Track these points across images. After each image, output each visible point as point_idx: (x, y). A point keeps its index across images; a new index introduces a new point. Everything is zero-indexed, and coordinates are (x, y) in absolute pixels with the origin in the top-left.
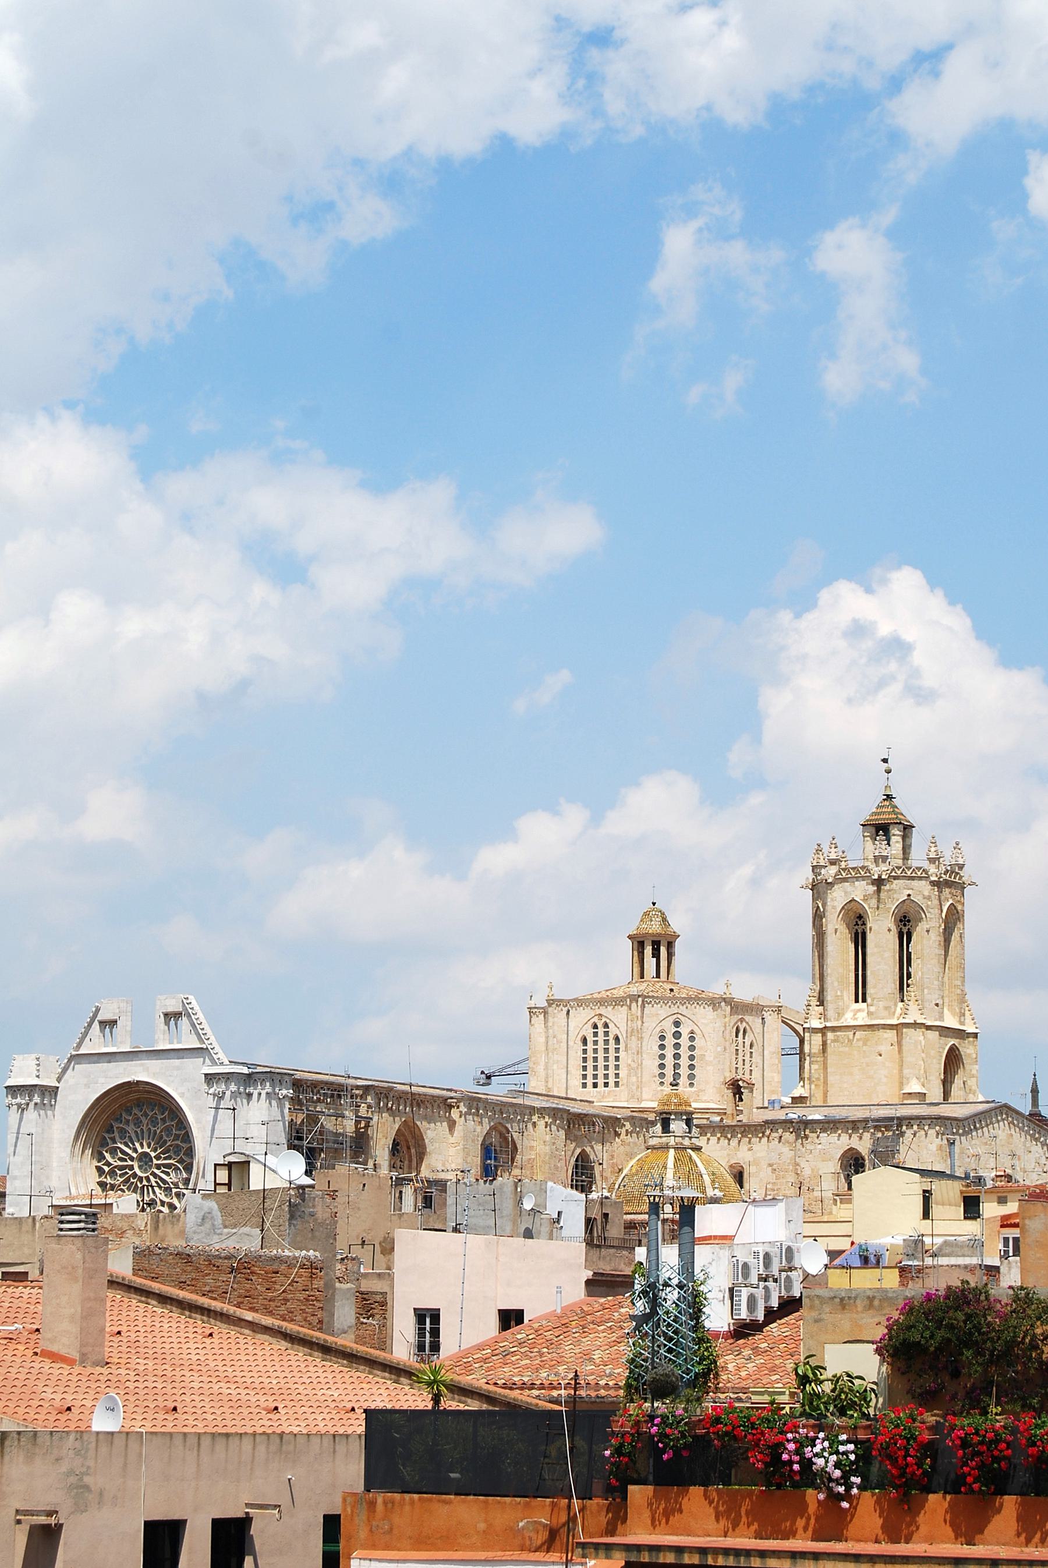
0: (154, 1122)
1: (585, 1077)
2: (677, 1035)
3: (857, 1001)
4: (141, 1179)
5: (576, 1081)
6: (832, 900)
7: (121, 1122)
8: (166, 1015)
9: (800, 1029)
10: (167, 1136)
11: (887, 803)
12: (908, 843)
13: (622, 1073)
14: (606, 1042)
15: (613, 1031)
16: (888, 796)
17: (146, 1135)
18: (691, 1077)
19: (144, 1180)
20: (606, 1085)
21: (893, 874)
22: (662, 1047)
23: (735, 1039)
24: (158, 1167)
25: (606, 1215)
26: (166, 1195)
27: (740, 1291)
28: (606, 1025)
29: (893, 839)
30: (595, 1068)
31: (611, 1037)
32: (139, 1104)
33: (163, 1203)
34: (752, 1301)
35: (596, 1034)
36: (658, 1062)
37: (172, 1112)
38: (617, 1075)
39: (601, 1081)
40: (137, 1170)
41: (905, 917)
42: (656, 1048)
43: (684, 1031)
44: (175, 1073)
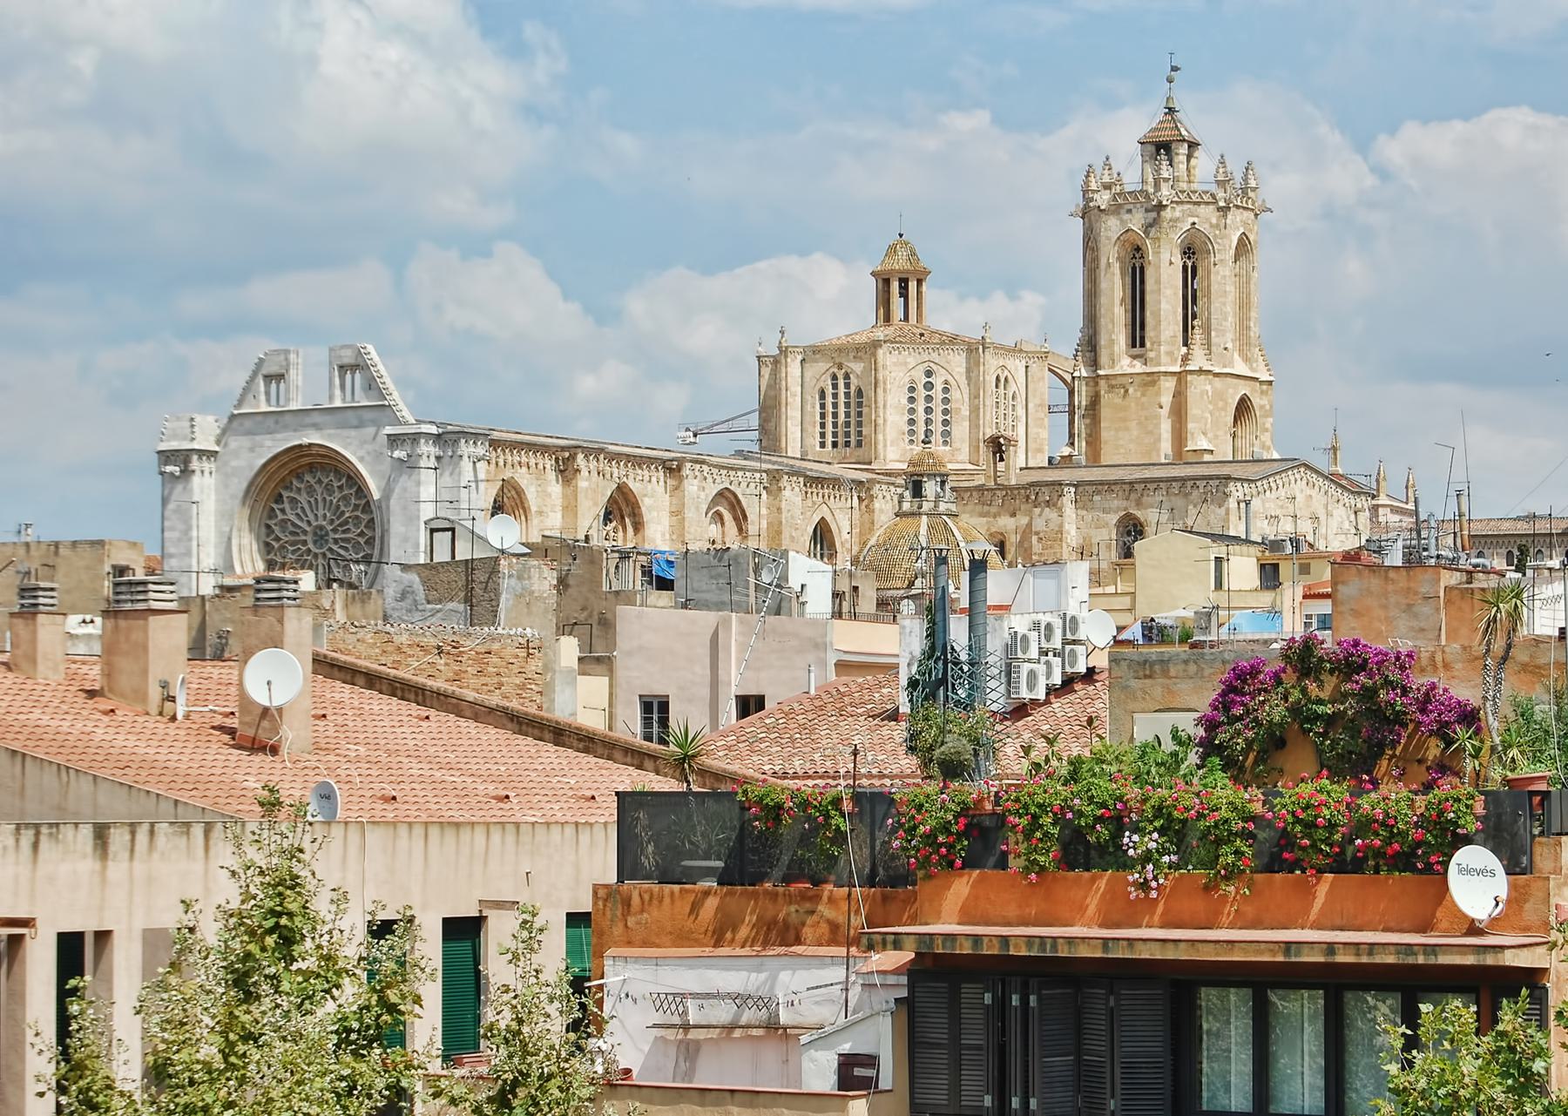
0: (329, 489)
2: (929, 386)
3: (1134, 346)
4: (316, 556)
6: (1106, 229)
7: (291, 490)
8: (341, 367)
9: (1068, 378)
10: (345, 506)
14: (847, 395)
16: (1170, 109)
17: (321, 505)
18: (946, 434)
19: (320, 556)
21: (1176, 199)
22: (912, 400)
23: (995, 390)
24: (336, 541)
25: (856, 589)
27: (1019, 667)
32: (311, 468)
35: (835, 386)
36: (906, 417)
37: (349, 477)
40: (311, 546)
41: (1189, 249)
42: (904, 401)
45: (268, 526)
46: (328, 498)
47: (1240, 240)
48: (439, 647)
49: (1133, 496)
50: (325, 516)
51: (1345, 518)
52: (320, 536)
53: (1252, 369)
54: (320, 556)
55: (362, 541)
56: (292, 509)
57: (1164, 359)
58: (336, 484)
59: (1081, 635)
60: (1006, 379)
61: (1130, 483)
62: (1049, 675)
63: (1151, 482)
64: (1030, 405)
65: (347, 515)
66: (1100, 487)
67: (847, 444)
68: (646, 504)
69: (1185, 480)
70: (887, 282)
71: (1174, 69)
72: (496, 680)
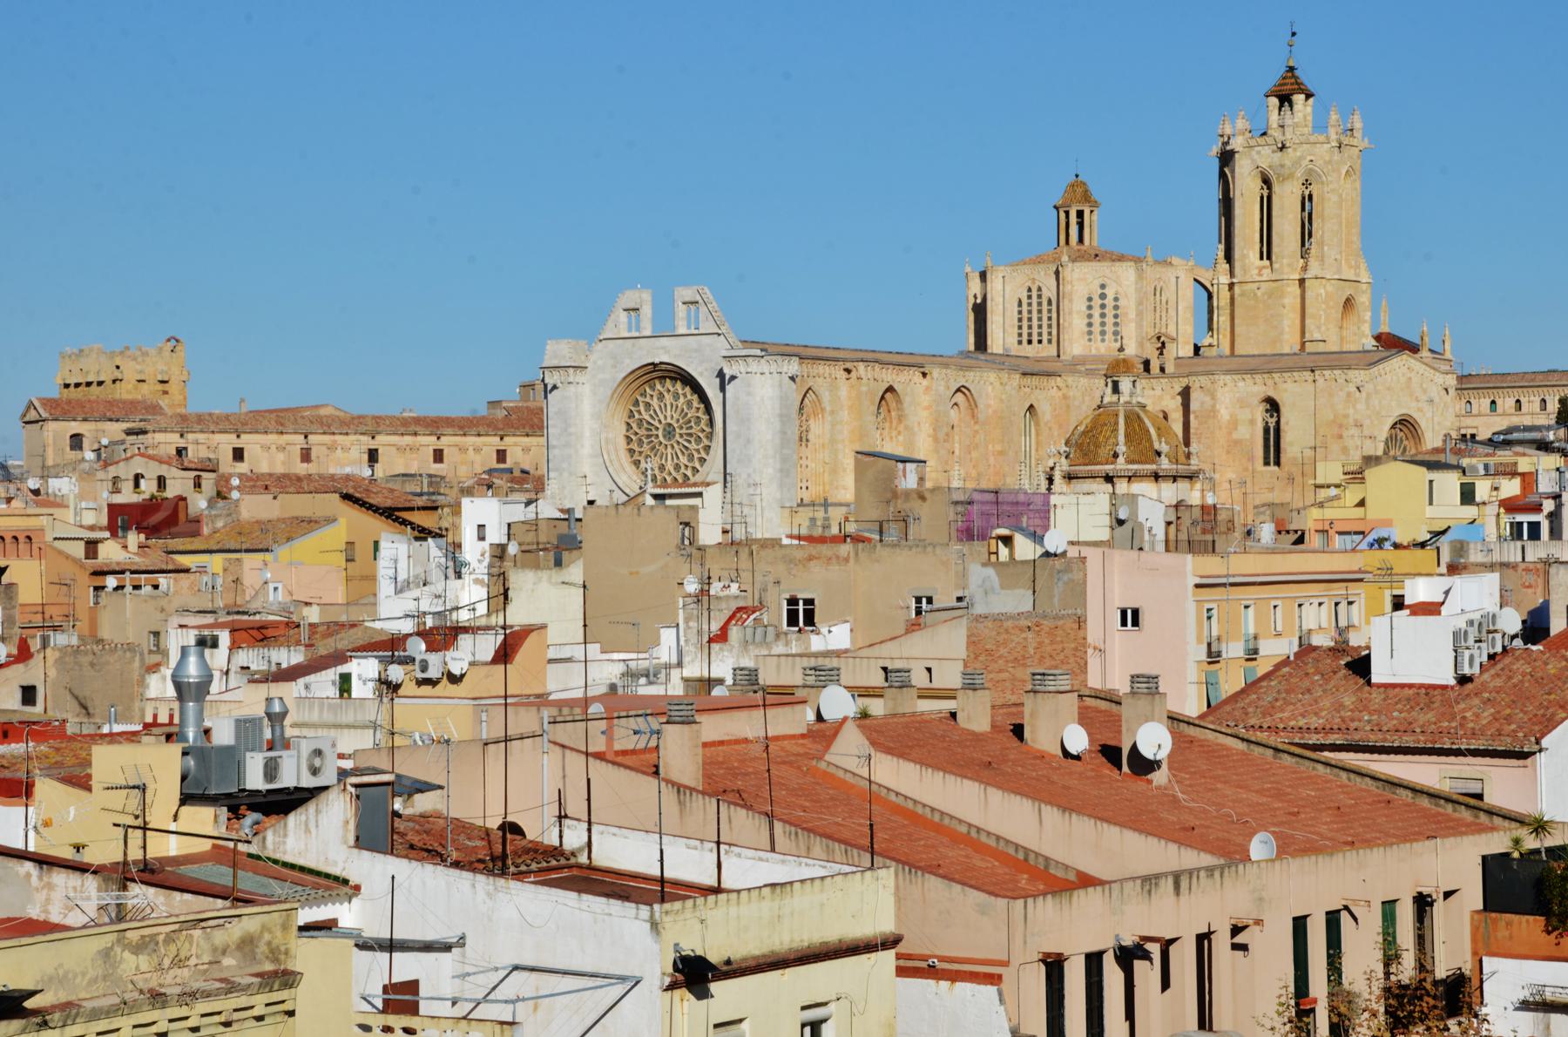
1: (1020, 335)
2: (1103, 296)
9: (1209, 286)
11: (1289, 74)
14: (1040, 304)
15: (1046, 294)
17: (669, 407)
19: (669, 447)
20: (1040, 342)
22: (1090, 307)
28: (1039, 289)
29: (1296, 107)
35: (1030, 297)
36: (1086, 321)
39: (1035, 338)
40: (661, 439)
41: (1307, 180)
42: (1084, 308)
45: (628, 424)
50: (678, 421)
52: (669, 431)
54: (669, 447)
57: (1286, 270)
59: (1498, 627)
64: (1180, 308)
72: (1060, 646)
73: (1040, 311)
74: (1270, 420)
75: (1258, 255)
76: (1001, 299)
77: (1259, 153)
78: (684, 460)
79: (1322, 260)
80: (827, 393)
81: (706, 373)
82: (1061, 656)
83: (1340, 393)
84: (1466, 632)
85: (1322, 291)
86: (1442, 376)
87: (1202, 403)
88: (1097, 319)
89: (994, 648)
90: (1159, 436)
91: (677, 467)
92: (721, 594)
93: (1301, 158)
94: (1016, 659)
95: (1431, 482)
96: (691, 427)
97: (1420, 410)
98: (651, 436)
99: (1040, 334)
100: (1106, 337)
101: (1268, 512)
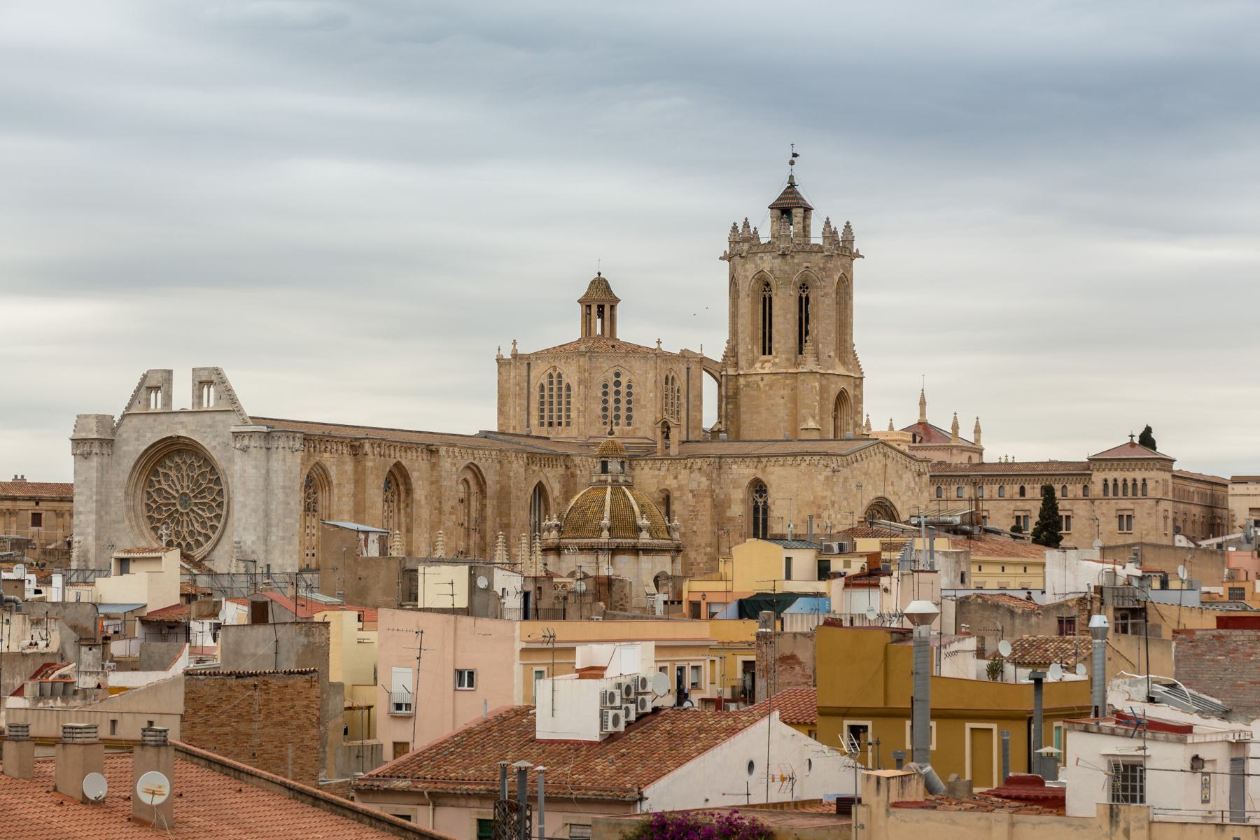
0: (191, 466)
1: (542, 417)
2: (618, 384)
3: (764, 353)
4: (182, 514)
5: (535, 421)
8: (201, 383)
12: (807, 222)
13: (573, 414)
14: (560, 389)
15: (565, 380)
17: (185, 479)
18: (629, 418)
20: (560, 424)
21: (795, 250)
22: (605, 394)
23: (664, 386)
24: (196, 504)
25: (540, 588)
26: (202, 528)
28: (560, 376)
29: (795, 220)
30: (551, 410)
31: (564, 386)
32: (179, 452)
33: (200, 533)
34: (616, 720)
35: (551, 383)
36: (601, 406)
37: (205, 460)
38: (568, 417)
40: (178, 507)
41: (804, 285)
42: (600, 394)
43: (624, 380)
44: (209, 430)
45: (148, 493)
46: (191, 474)
47: (840, 278)
48: (255, 686)
49: (760, 466)
51: (912, 479)
53: (848, 370)
55: (214, 504)
56: (165, 481)
58: (196, 464)
60: (673, 378)
61: (758, 457)
62: (627, 715)
63: (772, 456)
64: (690, 396)
65: (204, 486)
66: (737, 459)
67: (560, 424)
68: (414, 475)
69: (797, 456)
70: (589, 307)
71: (795, 155)
72: (291, 703)
73: (560, 396)
74: (759, 500)
75: (761, 350)
76: (526, 384)
77: (761, 258)
78: (198, 527)
79: (817, 357)
80: (334, 468)
81: (218, 447)
82: (291, 712)
83: (820, 477)
84: (612, 695)
85: (817, 384)
86: (916, 464)
87: (699, 483)
88: (611, 404)
89: (216, 704)
90: (642, 513)
91: (191, 533)
92: (28, 651)
93: (799, 264)
94: (240, 714)
95: (789, 560)
96: (205, 497)
97: (895, 493)
98: (169, 504)
99: (560, 417)
100: (620, 421)
101: (670, 584)
